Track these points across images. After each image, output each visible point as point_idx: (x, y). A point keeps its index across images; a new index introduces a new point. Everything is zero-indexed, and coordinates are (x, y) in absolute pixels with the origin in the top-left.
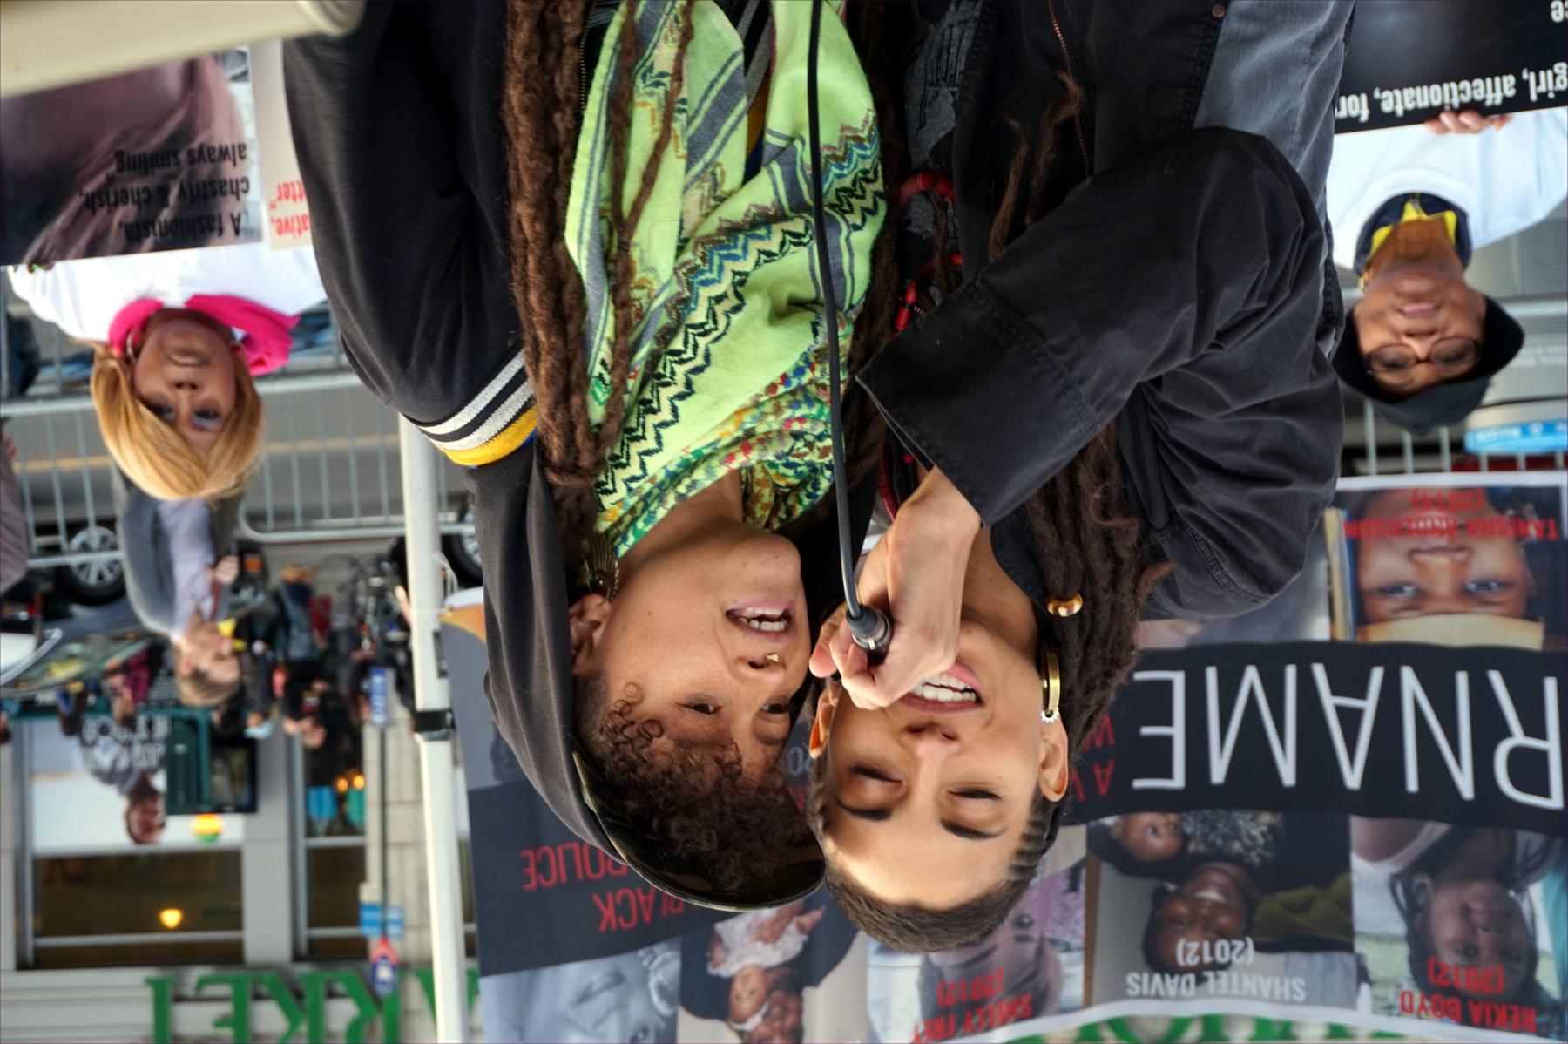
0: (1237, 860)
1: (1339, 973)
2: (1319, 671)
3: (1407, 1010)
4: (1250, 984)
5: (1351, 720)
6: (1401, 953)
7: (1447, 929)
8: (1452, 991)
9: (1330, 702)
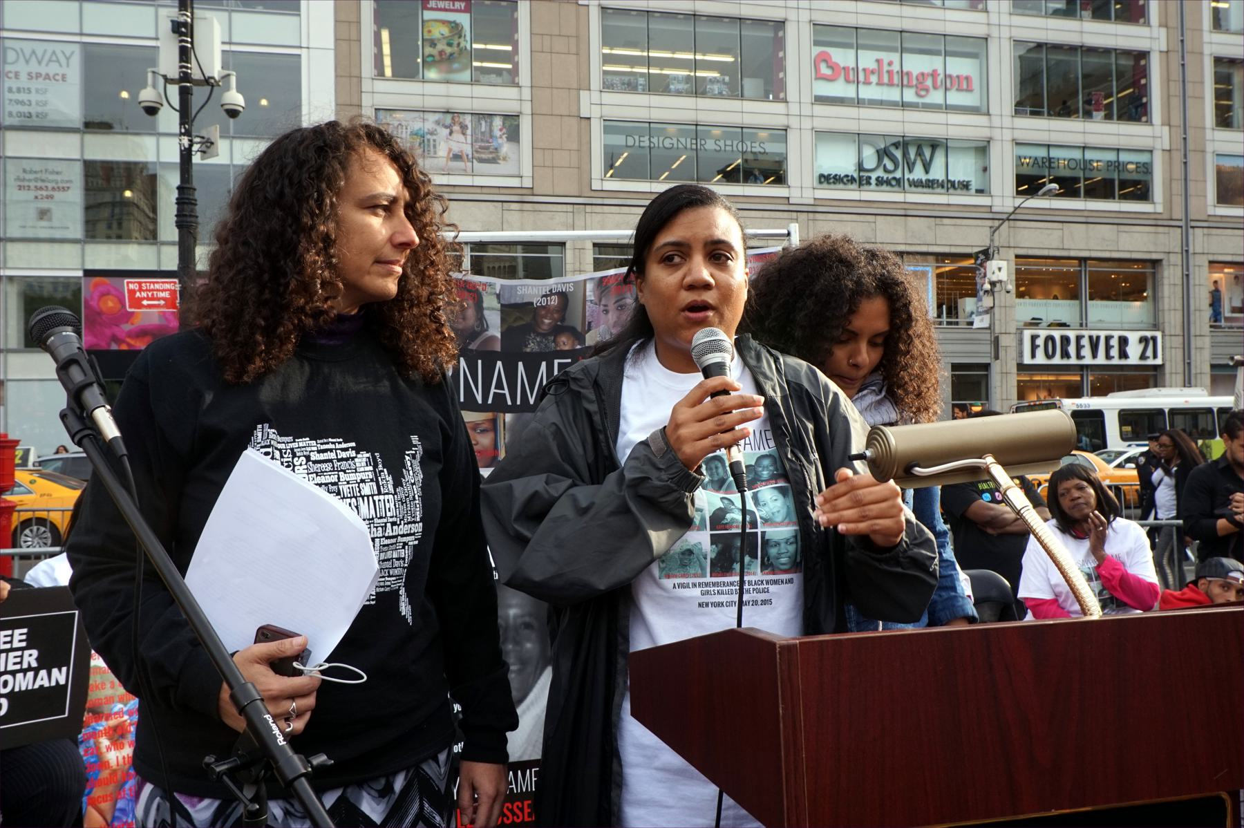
0: (538, 334)
1: (506, 296)
2: (509, 403)
3: (485, 285)
4: (536, 291)
5: (499, 385)
6: (485, 305)
7: (471, 313)
8: (469, 291)
9: (506, 392)
